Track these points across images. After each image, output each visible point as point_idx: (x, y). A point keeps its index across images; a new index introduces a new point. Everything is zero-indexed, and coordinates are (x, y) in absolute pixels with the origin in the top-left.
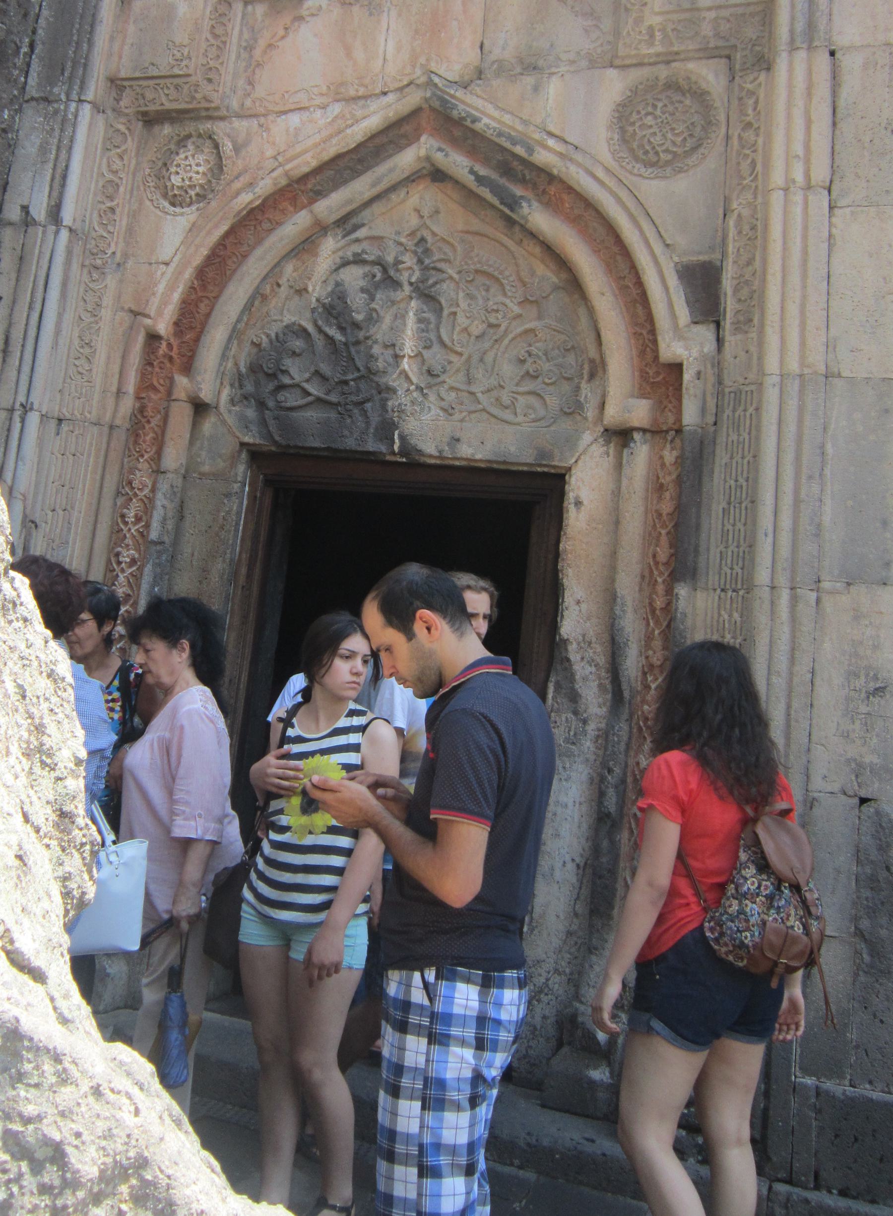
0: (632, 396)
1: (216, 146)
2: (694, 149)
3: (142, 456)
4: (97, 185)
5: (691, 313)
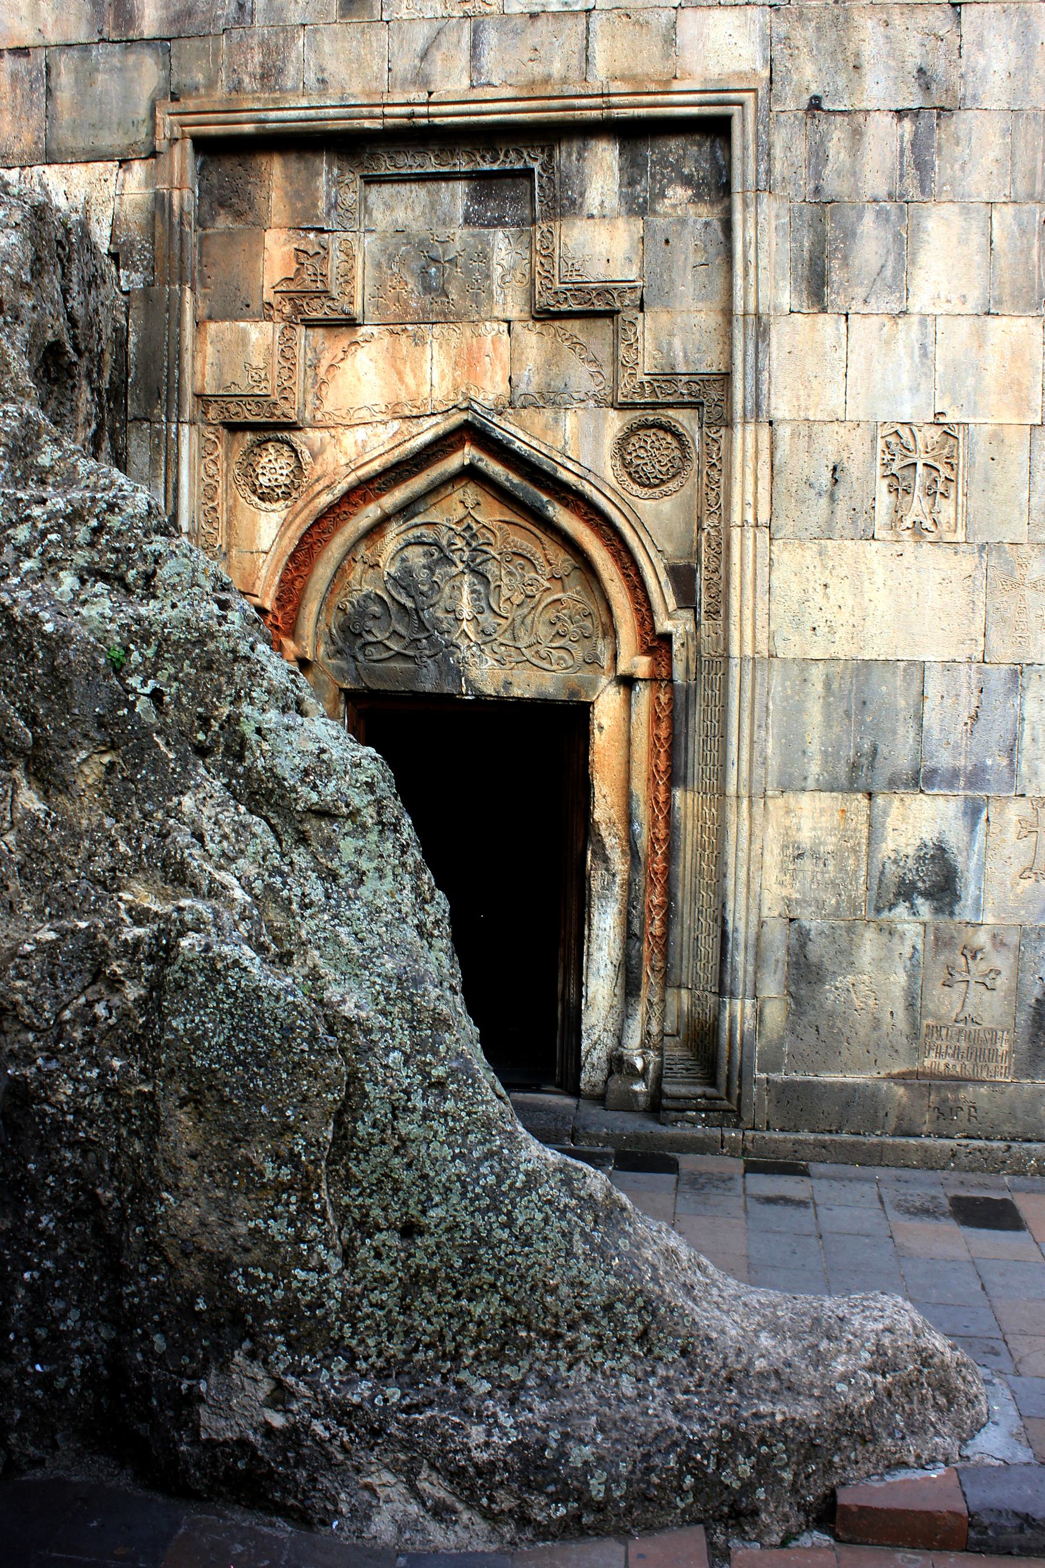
0: (636, 655)
2: (674, 476)
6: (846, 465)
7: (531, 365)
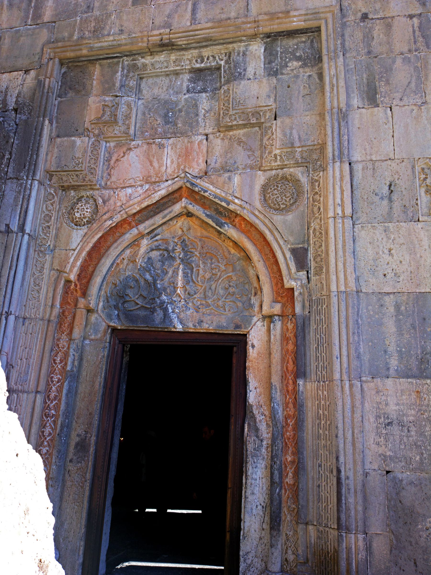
1: (95, 201)
3: (64, 333)
4: (41, 216)
5: (297, 268)
6: (397, 182)
7: (217, 154)
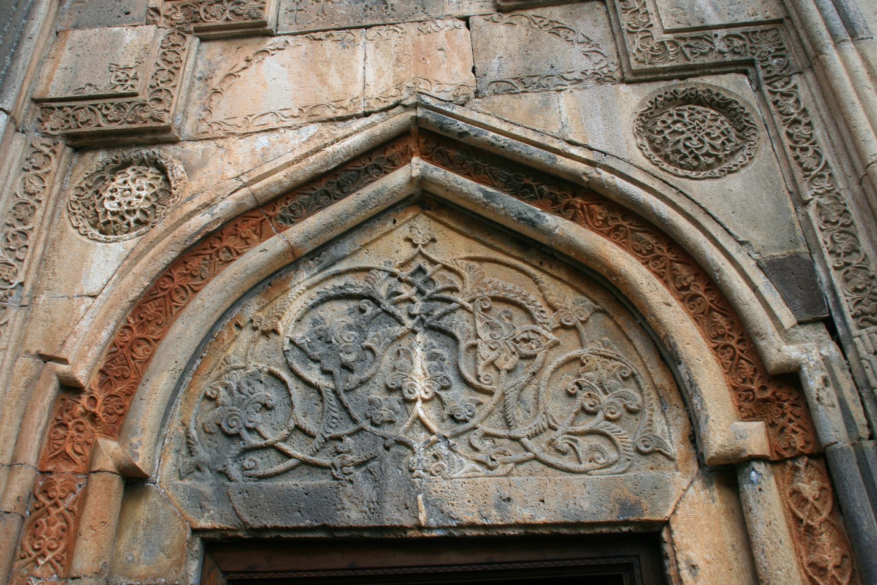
1: (162, 170)
